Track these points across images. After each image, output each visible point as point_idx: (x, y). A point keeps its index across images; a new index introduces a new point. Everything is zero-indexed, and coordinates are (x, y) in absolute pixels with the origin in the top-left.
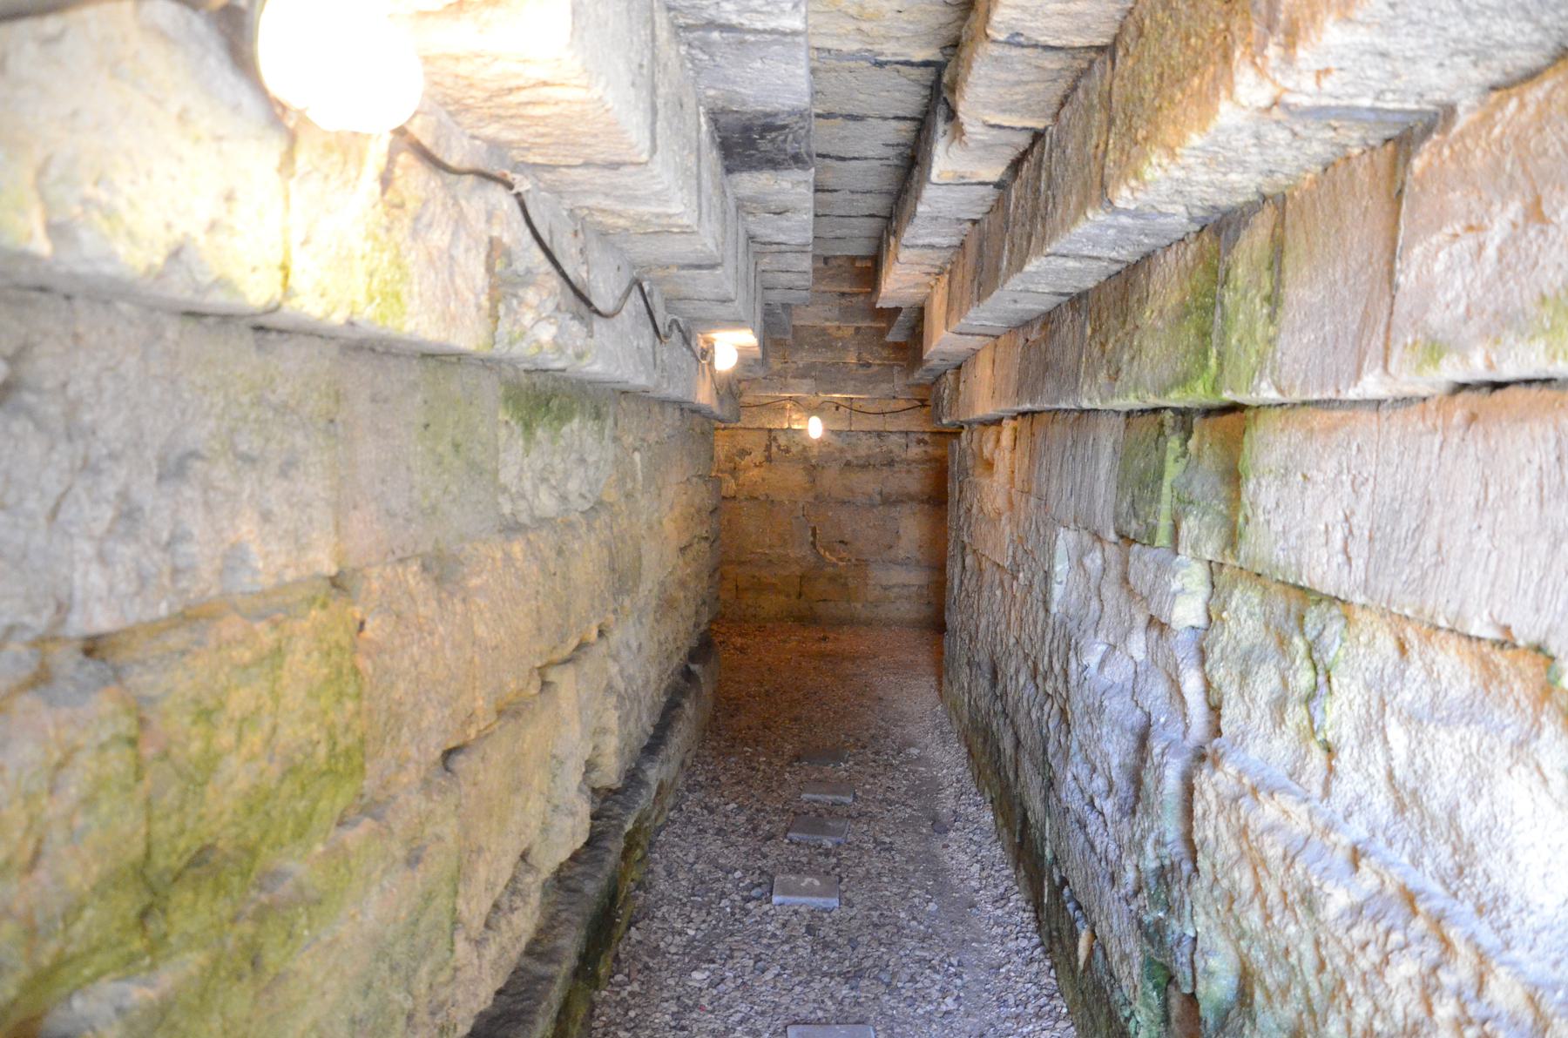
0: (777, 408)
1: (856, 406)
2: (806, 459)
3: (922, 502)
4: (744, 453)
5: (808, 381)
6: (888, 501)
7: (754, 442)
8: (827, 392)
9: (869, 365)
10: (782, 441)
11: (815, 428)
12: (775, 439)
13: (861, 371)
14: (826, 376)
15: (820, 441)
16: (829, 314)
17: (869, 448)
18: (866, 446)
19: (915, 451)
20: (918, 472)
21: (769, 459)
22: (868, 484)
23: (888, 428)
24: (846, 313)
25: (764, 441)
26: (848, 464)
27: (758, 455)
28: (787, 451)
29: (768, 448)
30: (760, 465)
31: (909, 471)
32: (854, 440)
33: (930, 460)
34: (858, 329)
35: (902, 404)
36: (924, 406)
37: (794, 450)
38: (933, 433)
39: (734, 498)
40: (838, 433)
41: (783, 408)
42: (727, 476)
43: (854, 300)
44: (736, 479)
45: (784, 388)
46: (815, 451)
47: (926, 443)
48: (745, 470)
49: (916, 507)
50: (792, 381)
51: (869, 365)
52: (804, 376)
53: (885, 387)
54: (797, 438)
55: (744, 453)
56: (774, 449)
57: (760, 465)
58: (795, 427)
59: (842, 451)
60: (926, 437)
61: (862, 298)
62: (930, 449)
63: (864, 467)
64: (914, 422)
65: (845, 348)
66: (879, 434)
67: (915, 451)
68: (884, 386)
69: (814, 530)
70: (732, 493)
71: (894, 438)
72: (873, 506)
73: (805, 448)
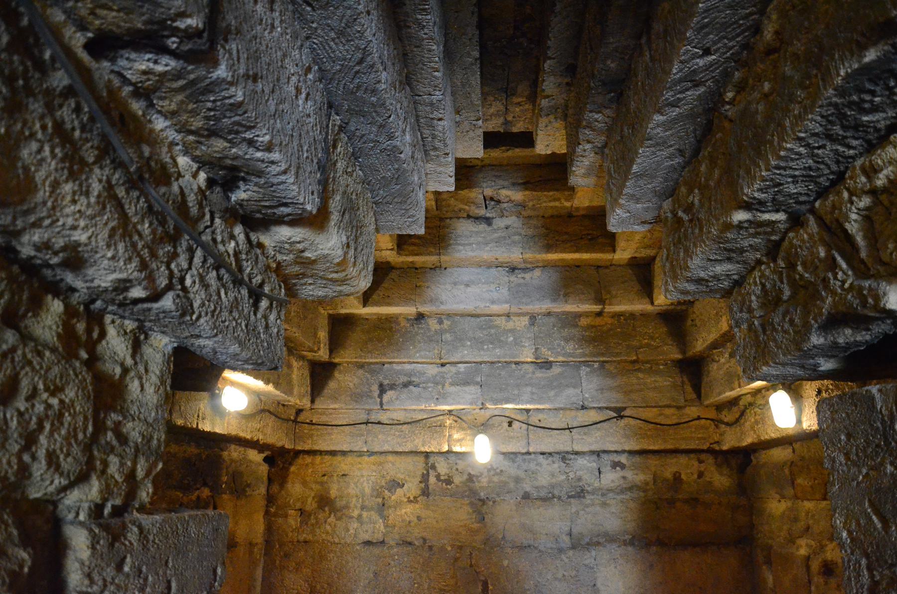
0: (431, 424)
1: (534, 420)
2: (473, 493)
3: (625, 543)
4: (395, 484)
5: (473, 389)
6: (579, 544)
7: (407, 470)
8: (496, 402)
9: (547, 365)
10: (442, 468)
11: (482, 450)
12: (433, 467)
13: (540, 374)
14: (493, 378)
15: (490, 469)
16: (495, 295)
17: (553, 475)
18: (547, 473)
19: (611, 478)
20: (614, 501)
21: (425, 492)
22: (551, 522)
23: (577, 448)
24: (518, 293)
25: (418, 465)
26: (526, 496)
27: (412, 488)
28: (449, 481)
29: (425, 478)
30: (415, 500)
31: (604, 505)
32: (532, 466)
33: (630, 489)
34: (533, 318)
35: (594, 416)
36: (622, 417)
37: (457, 480)
38: (631, 453)
39: (383, 542)
40: (511, 456)
41: (442, 425)
42: (374, 516)
43: (528, 276)
44: (385, 518)
45: (441, 398)
46: (484, 481)
47: (623, 467)
48: (398, 505)
49: (615, 550)
50: (453, 389)
51: (547, 365)
52: (466, 383)
53: (570, 395)
54: (461, 465)
55: (395, 484)
56: (432, 480)
57: (415, 500)
58: (457, 449)
59: (517, 480)
60: (623, 459)
61: (537, 273)
62: (629, 474)
63: (547, 499)
64: (614, 438)
65: (517, 343)
66: (564, 456)
67: (611, 478)
68: (571, 391)
69: (485, 584)
70: (379, 537)
71: (582, 461)
72: (561, 551)
73: (471, 478)
